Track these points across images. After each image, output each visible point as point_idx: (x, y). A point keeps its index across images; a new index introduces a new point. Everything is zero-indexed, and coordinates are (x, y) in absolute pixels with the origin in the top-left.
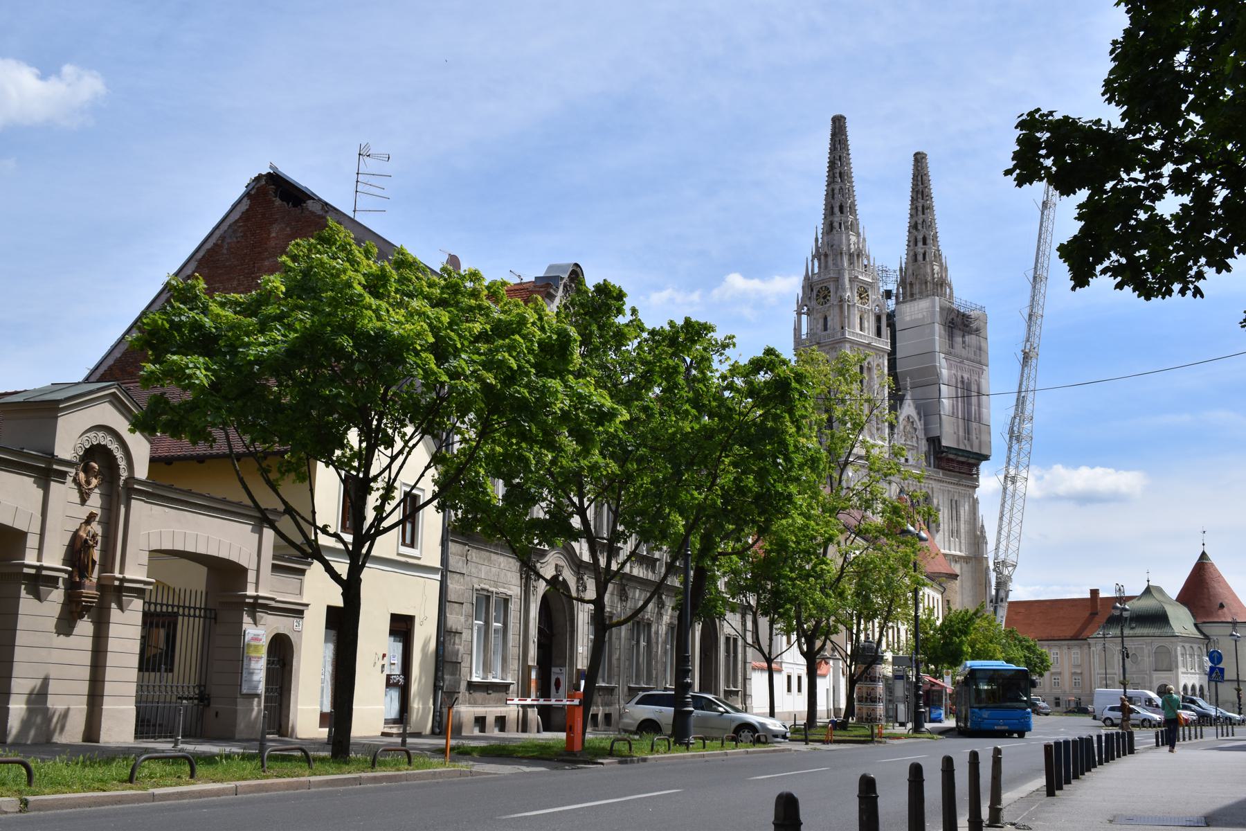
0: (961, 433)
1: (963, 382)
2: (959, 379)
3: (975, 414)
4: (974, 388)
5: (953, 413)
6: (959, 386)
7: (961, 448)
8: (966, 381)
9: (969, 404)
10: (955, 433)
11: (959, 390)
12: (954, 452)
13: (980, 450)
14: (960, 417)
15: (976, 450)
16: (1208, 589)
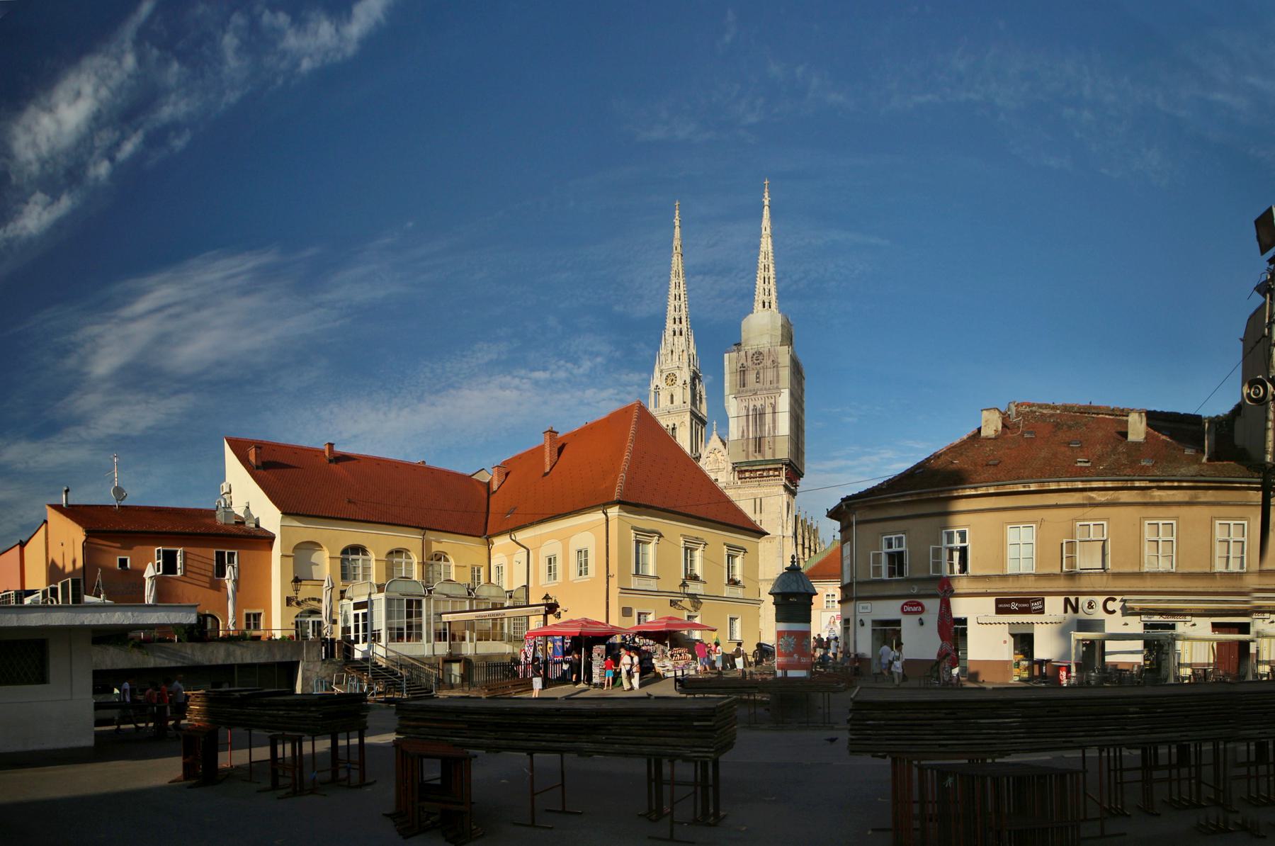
0: (751, 448)
1: (755, 409)
2: (751, 407)
3: (769, 427)
4: (769, 410)
5: (743, 436)
6: (751, 413)
7: (750, 460)
8: (759, 406)
9: (762, 424)
10: (744, 451)
11: (750, 417)
12: (745, 464)
13: (774, 454)
14: (751, 436)
15: (768, 456)
16: (1199, 484)
